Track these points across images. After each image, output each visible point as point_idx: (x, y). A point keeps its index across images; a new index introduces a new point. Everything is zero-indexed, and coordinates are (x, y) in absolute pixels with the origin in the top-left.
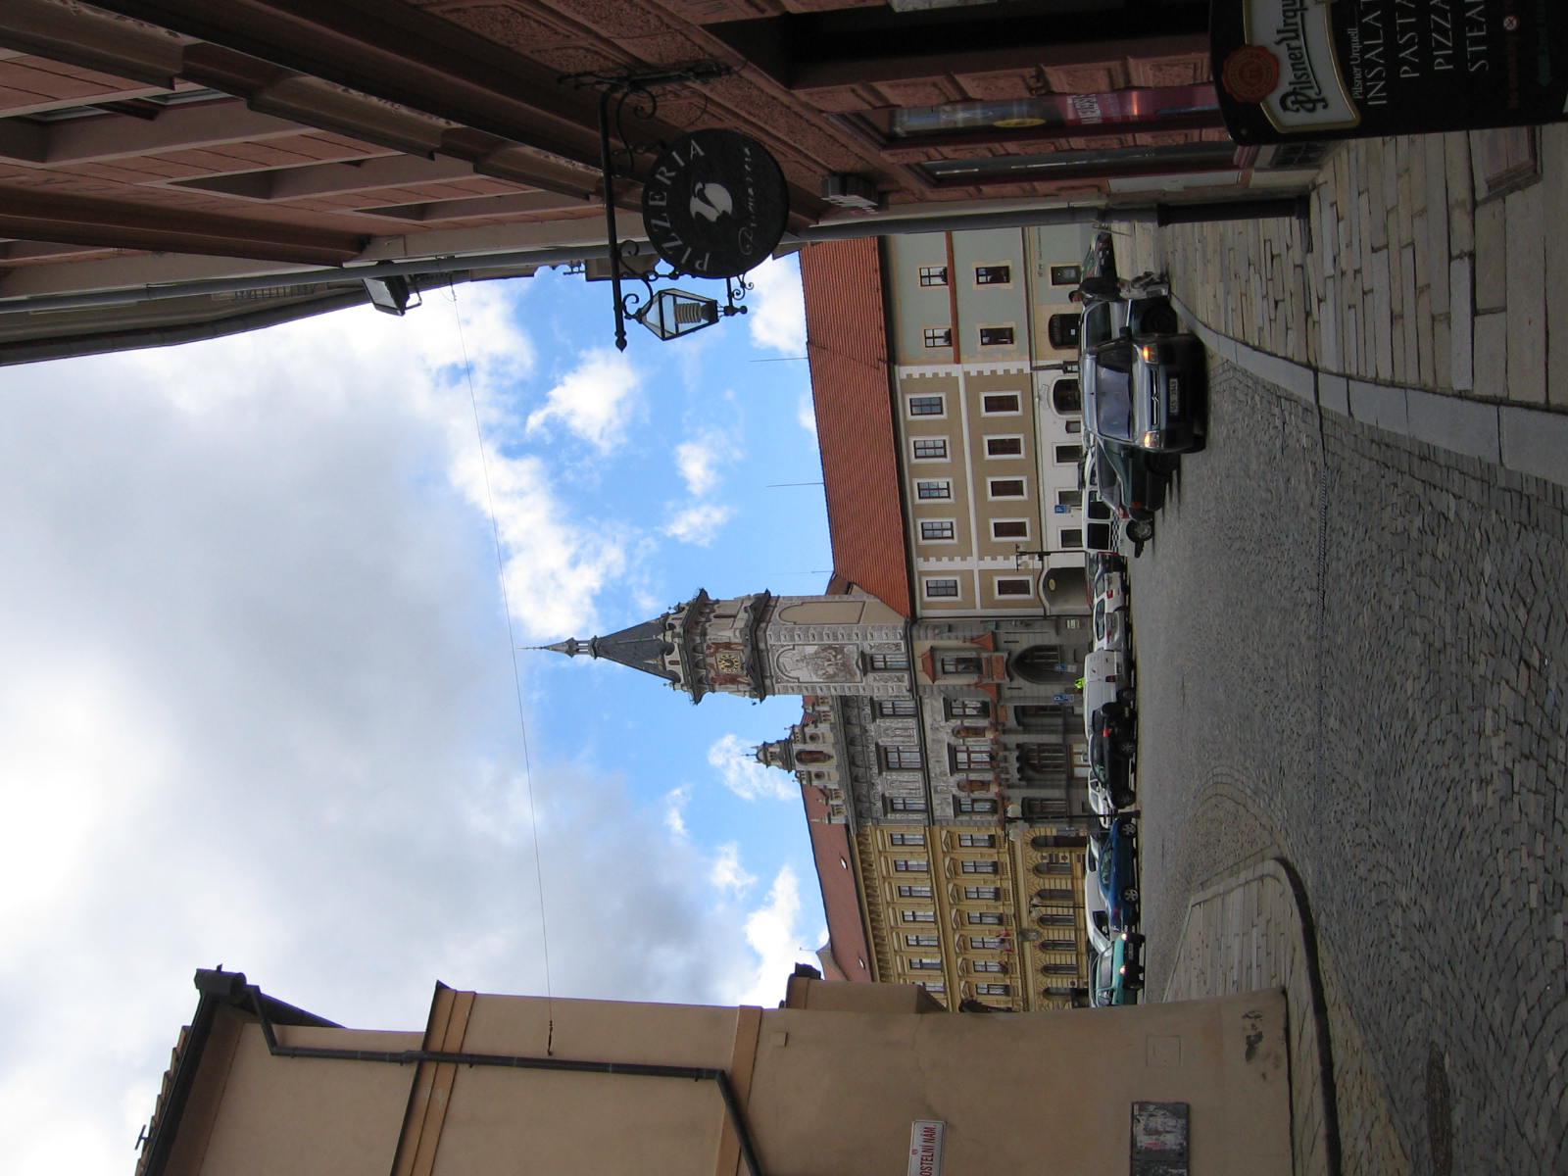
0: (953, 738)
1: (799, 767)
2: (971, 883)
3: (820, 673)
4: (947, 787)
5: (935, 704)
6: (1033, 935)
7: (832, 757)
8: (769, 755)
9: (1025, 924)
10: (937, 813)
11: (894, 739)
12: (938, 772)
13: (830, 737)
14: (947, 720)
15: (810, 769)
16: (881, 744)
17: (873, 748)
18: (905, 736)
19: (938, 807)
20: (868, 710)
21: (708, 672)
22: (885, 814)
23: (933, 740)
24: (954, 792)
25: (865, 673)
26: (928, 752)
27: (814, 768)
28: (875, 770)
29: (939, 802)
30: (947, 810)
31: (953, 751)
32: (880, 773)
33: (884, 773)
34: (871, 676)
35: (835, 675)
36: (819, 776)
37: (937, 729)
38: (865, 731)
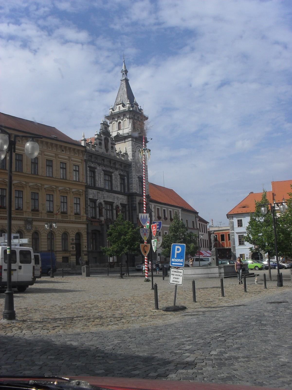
0: (115, 205)
1: (103, 137)
2: (57, 199)
3: (137, 161)
4: (100, 198)
5: (125, 201)
6: (29, 227)
7: (107, 152)
8: (106, 126)
9: (35, 223)
10: (90, 191)
11: (114, 181)
12: (105, 196)
13: (113, 154)
14: (121, 204)
15: (103, 141)
16: (113, 174)
17: (111, 170)
18: (115, 186)
19: (92, 192)
20: (122, 173)
21: (136, 120)
22: (89, 167)
23: (114, 196)
24: (98, 200)
25: (138, 177)
26: (111, 193)
27: (103, 142)
28: (104, 168)
29: (94, 193)
30: (91, 195)
31: (111, 204)
32: (103, 170)
33: (103, 172)
34: (138, 179)
35: (137, 166)
36: (100, 144)
37: (118, 199)
38: (117, 169)
